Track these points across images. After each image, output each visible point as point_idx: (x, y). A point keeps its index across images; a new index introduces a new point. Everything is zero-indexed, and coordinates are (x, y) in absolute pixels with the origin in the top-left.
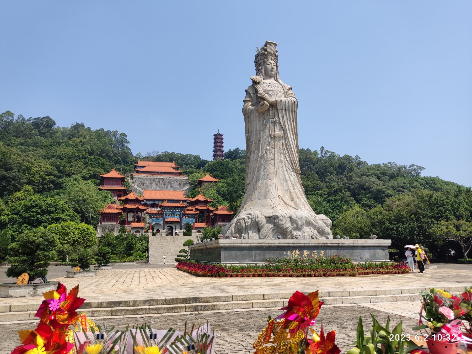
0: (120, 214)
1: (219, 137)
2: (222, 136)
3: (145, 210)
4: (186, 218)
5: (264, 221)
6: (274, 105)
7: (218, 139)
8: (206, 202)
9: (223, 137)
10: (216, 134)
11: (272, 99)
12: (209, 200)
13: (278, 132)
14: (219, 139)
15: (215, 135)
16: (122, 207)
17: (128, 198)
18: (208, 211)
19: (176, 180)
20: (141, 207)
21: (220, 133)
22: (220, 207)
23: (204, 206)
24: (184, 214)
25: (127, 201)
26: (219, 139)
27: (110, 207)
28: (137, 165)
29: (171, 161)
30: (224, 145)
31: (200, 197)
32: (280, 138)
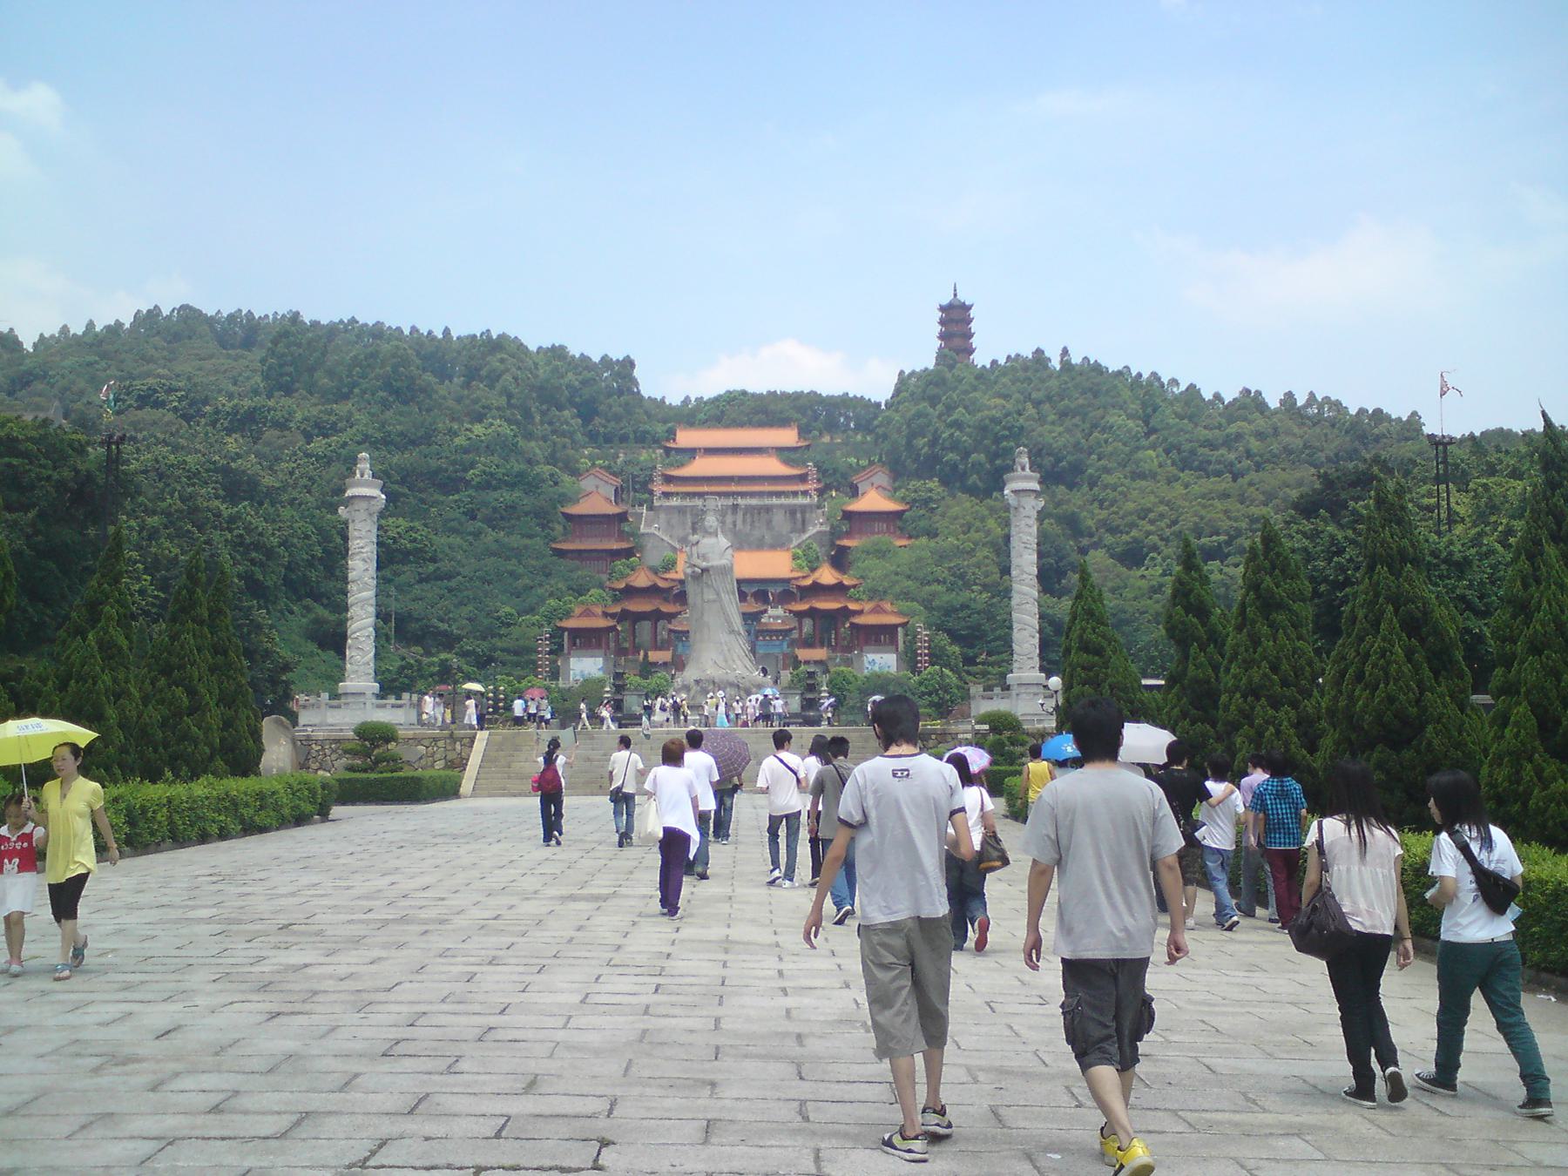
0: (613, 628)
1: (955, 315)
2: (966, 308)
3: (680, 613)
4: (764, 640)
5: (692, 683)
6: (705, 570)
7: (956, 320)
8: (839, 589)
9: (972, 313)
10: (945, 302)
11: (704, 564)
12: (846, 583)
13: (712, 596)
14: (957, 322)
15: (942, 309)
16: (617, 609)
17: (632, 584)
18: (846, 613)
19: (781, 506)
20: (666, 608)
21: (962, 297)
22: (868, 606)
23: (839, 602)
24: (759, 631)
25: (630, 592)
26: (957, 322)
27: (587, 613)
28: (672, 445)
29: (781, 422)
30: (975, 341)
31: (827, 576)
32: (714, 601)
